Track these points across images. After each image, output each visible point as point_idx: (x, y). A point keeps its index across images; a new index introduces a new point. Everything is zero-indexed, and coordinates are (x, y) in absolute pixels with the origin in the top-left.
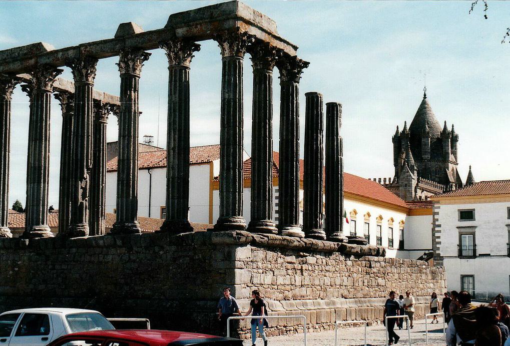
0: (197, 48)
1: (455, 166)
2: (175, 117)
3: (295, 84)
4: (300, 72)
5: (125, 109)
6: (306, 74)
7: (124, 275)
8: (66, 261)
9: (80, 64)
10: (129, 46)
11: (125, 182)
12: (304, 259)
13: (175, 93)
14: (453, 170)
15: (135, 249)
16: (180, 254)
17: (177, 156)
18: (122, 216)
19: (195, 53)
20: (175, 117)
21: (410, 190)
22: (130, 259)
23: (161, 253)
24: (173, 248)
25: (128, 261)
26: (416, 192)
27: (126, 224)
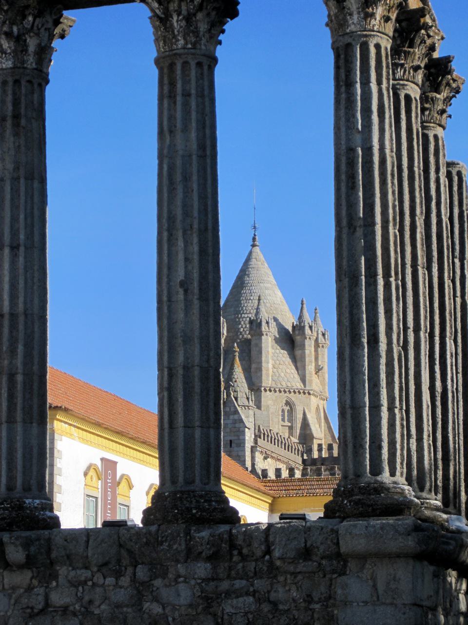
1: (322, 402)
2: (187, 192)
3: (439, 131)
4: (448, 100)
5: (17, 168)
11: (20, 378)
13: (185, 129)
14: (318, 409)
15: (63, 571)
16: (225, 585)
17: (196, 303)
20: (187, 192)
21: (240, 453)
22: (47, 604)
23: (158, 582)
24: (202, 569)
25: (42, 611)
26: (253, 458)
27: (27, 501)
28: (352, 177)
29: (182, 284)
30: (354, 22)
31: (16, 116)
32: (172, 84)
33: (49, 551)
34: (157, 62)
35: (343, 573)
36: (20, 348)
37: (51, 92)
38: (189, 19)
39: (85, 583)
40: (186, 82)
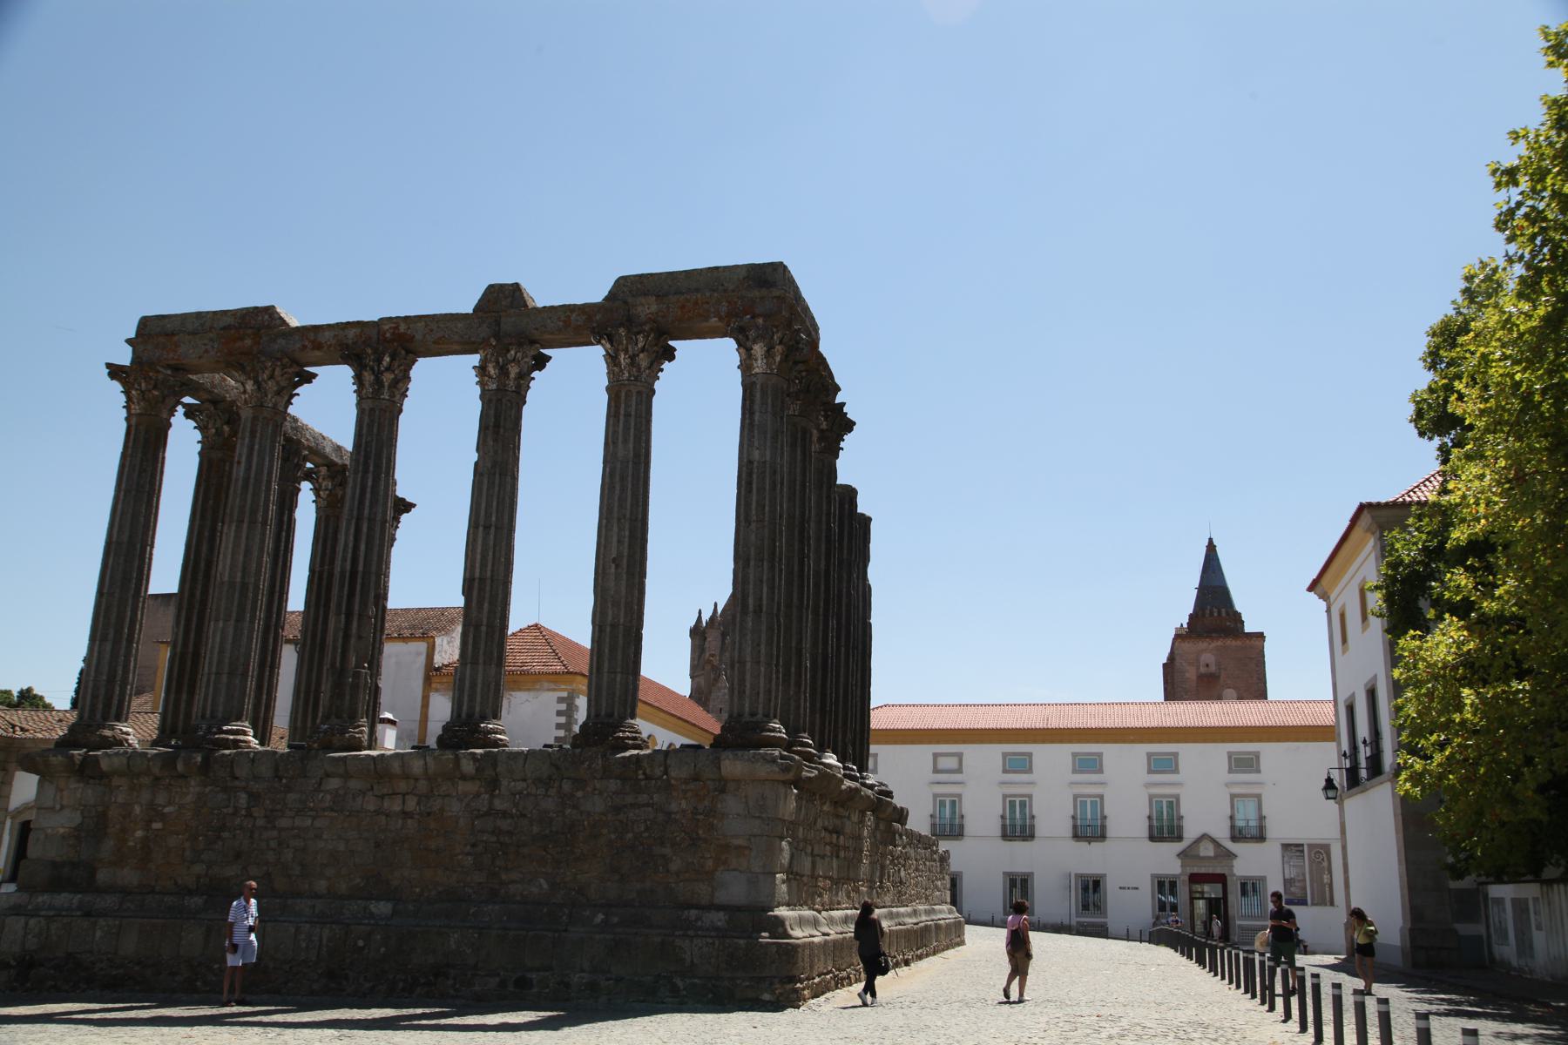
0: (670, 355)
6: (849, 442)
7: (473, 845)
8: (311, 809)
9: (379, 361)
10: (508, 336)
11: (484, 629)
12: (838, 822)
13: (626, 441)
15: (504, 782)
16: (629, 799)
18: (472, 708)
19: (666, 365)
20: (623, 490)
23: (579, 794)
24: (613, 785)
28: (749, 483)
29: (614, 560)
30: (759, 366)
31: (497, 426)
32: (617, 407)
33: (495, 765)
34: (608, 389)
35: (723, 791)
36: (486, 605)
37: (526, 411)
38: (633, 358)
39: (520, 793)
40: (627, 406)
